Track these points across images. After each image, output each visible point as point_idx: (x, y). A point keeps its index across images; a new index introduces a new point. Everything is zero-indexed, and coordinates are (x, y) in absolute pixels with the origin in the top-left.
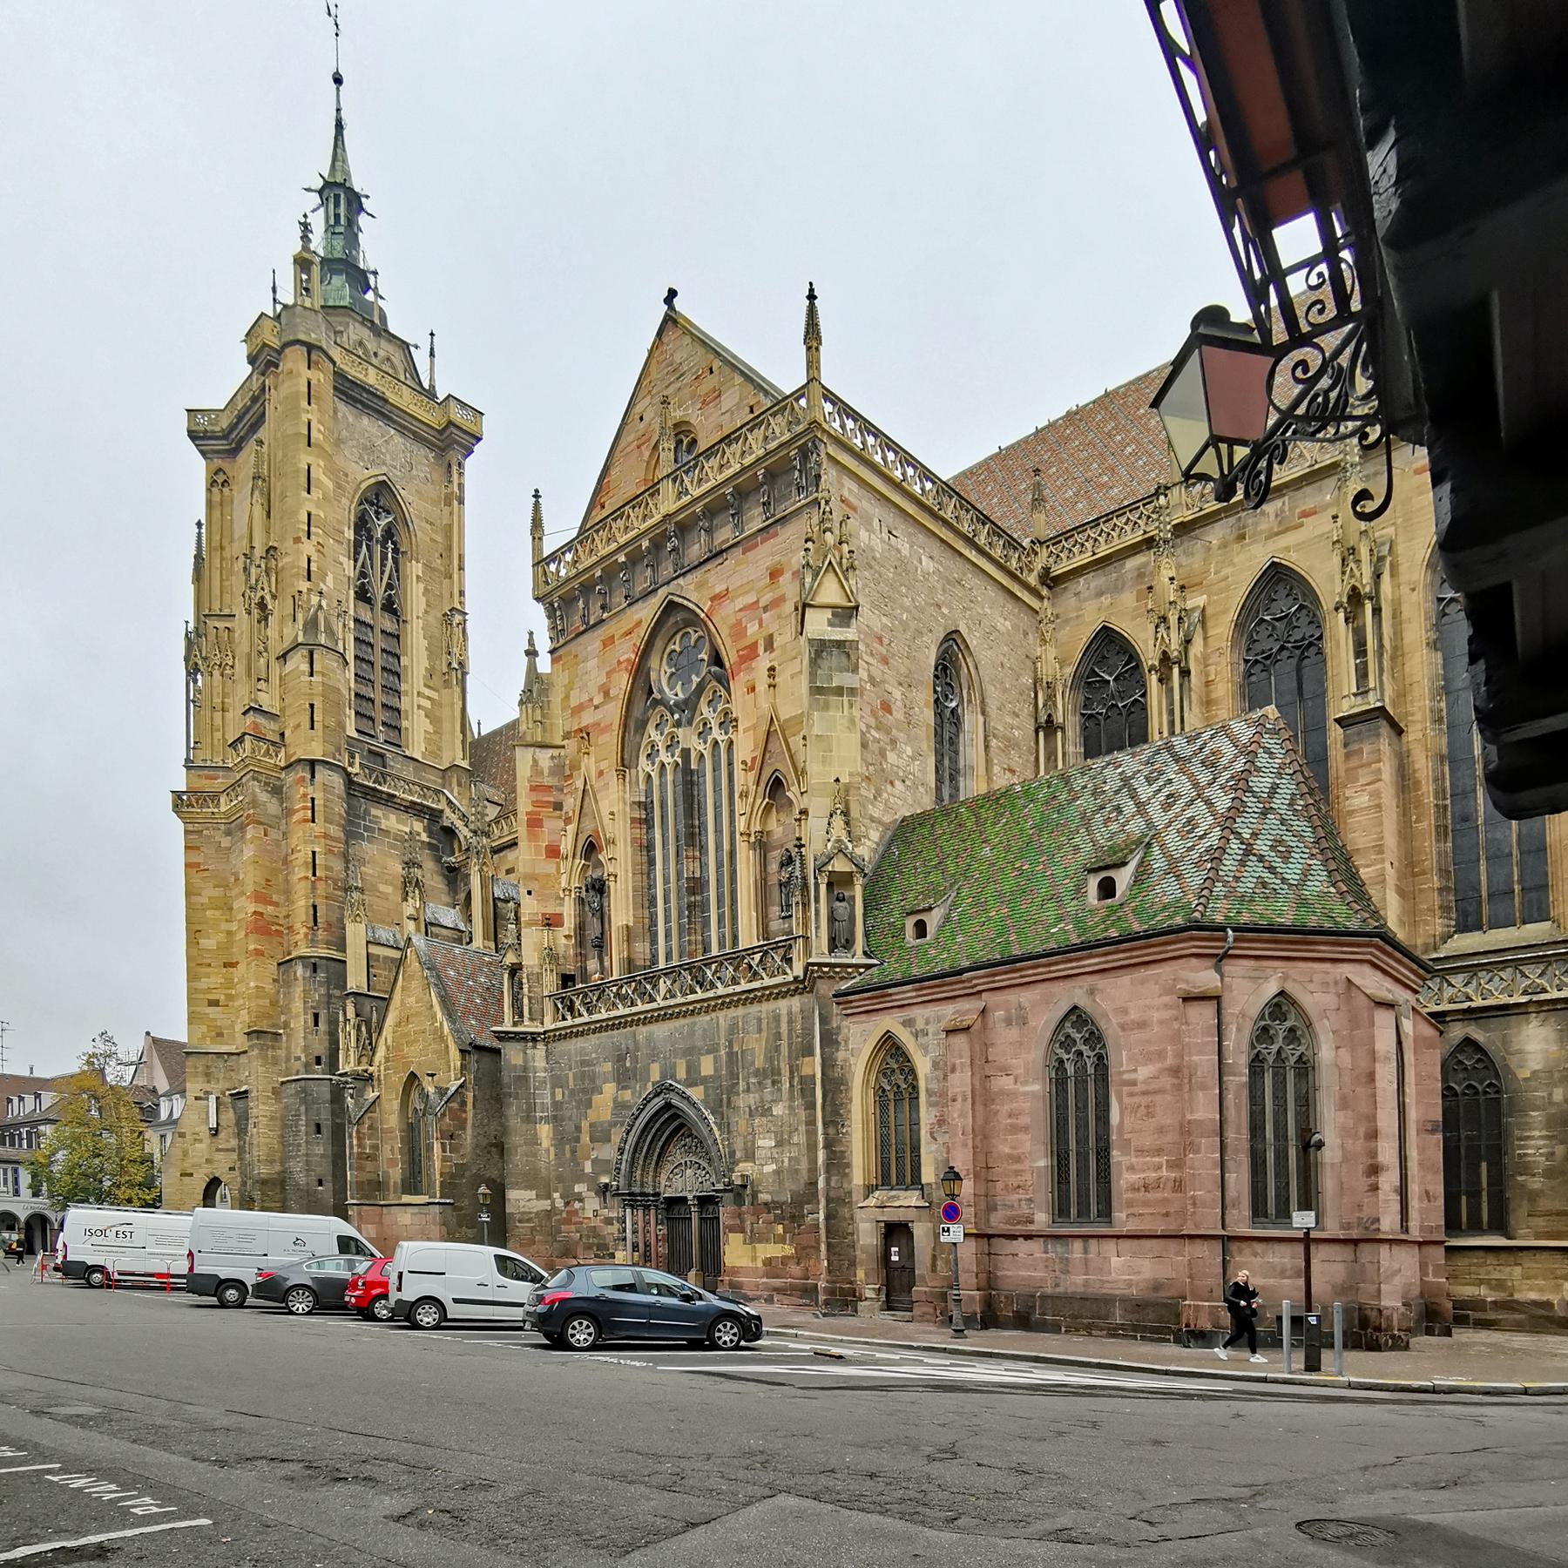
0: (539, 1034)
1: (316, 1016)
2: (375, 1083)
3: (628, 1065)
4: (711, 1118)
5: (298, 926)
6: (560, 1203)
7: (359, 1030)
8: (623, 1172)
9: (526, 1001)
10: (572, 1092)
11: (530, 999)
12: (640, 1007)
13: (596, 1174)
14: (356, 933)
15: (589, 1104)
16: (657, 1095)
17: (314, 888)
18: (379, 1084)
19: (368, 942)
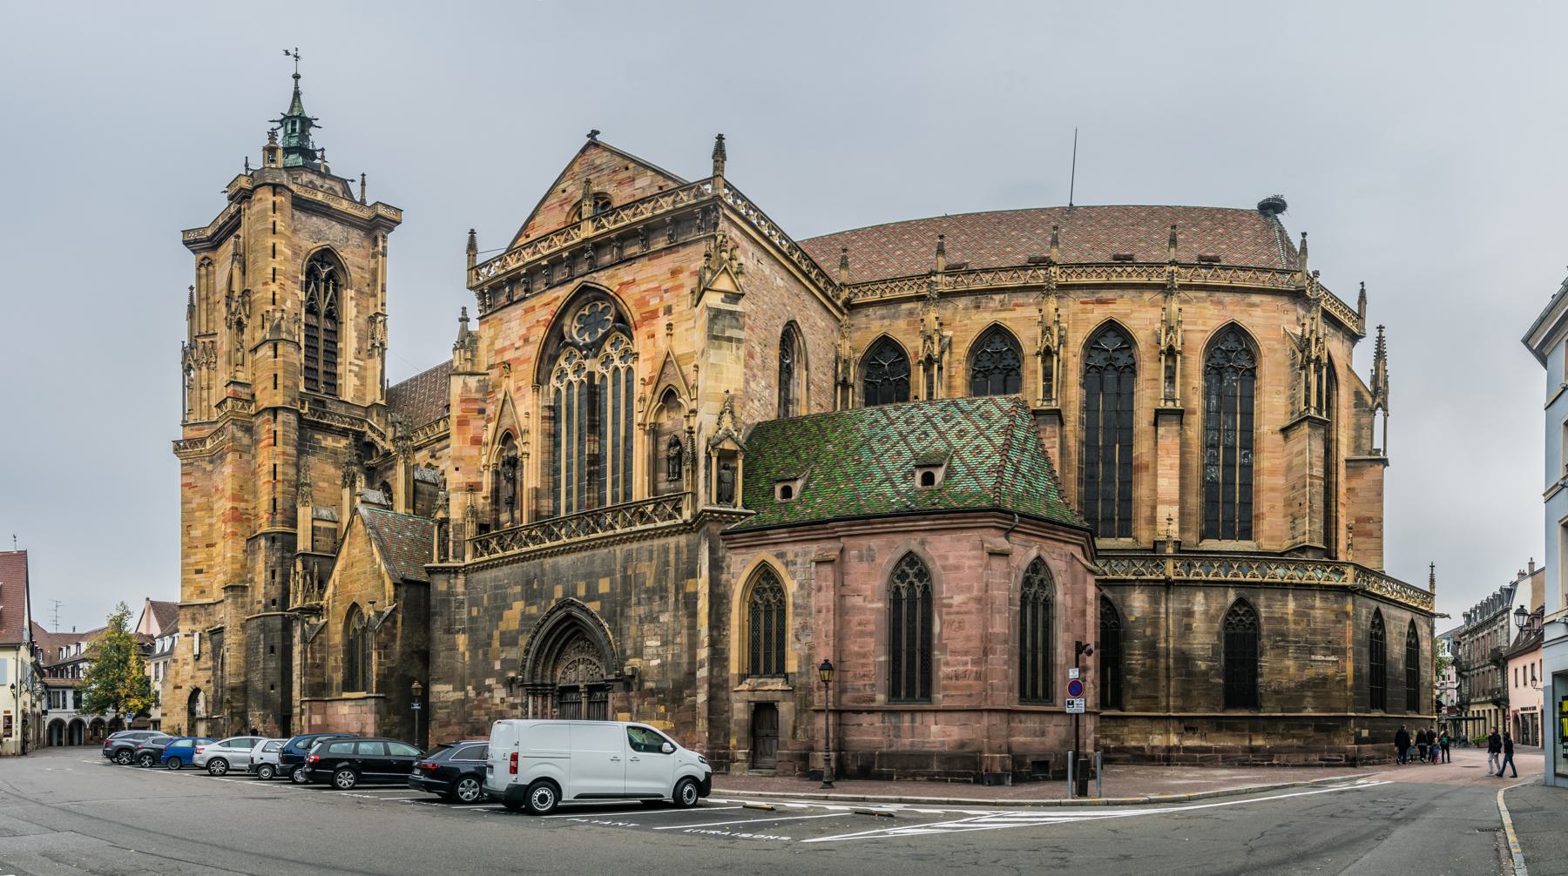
0: (460, 568)
1: (273, 573)
2: (325, 612)
3: (535, 587)
4: (606, 626)
5: (262, 513)
6: (472, 693)
7: (305, 579)
8: (527, 669)
9: (451, 544)
10: (486, 610)
11: (454, 542)
12: (548, 544)
13: (504, 670)
14: (304, 514)
15: (500, 618)
16: (560, 608)
17: (274, 487)
18: (328, 613)
19: (313, 519)
